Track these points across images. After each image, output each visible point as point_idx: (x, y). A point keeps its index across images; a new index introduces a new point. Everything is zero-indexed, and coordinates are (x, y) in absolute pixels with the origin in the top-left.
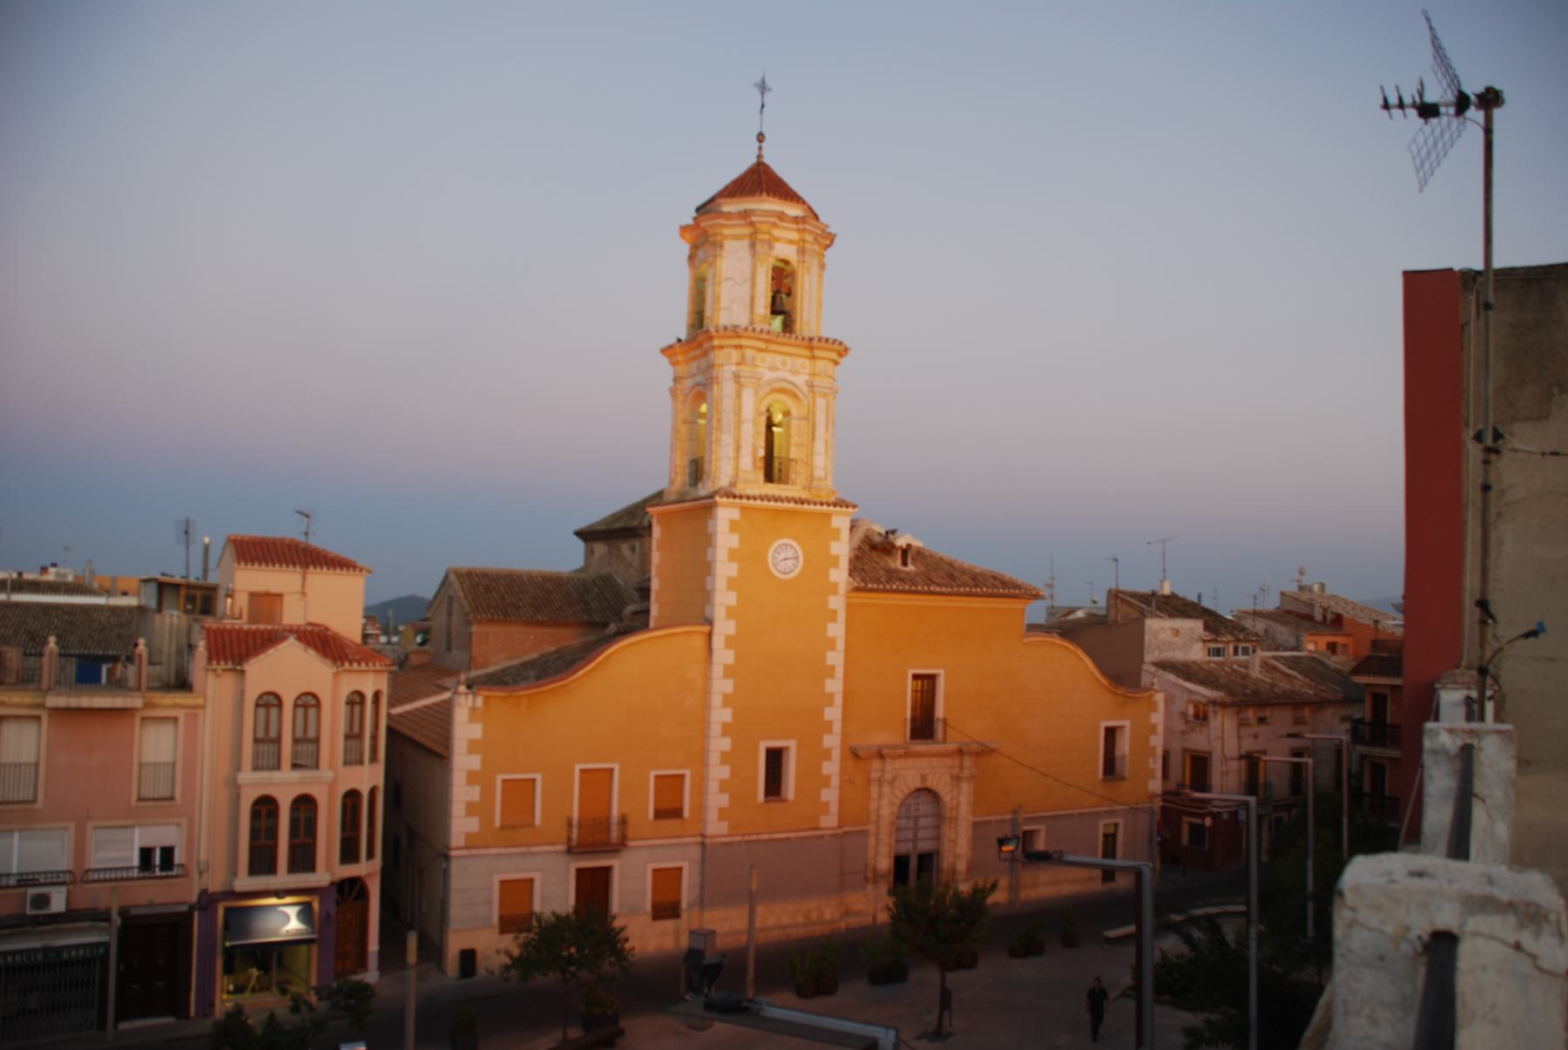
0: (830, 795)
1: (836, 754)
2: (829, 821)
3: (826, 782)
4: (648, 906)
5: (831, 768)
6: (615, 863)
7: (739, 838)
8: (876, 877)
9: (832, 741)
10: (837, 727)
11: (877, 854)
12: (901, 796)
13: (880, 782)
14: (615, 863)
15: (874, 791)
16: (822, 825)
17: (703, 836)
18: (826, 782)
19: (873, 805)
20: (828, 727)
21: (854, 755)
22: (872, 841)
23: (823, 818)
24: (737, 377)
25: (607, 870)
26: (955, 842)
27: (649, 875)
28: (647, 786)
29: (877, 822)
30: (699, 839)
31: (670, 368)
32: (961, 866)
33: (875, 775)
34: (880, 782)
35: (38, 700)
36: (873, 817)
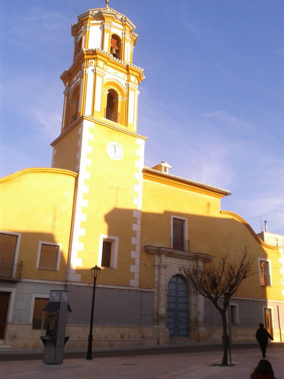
0: (135, 269)
1: (138, 248)
2: (134, 283)
3: (133, 262)
4: (31, 320)
5: (136, 255)
6: (14, 291)
7: (87, 285)
8: (158, 319)
9: (135, 241)
10: (138, 234)
11: (158, 306)
12: (170, 277)
13: (159, 267)
14: (14, 291)
15: (156, 271)
16: (131, 284)
17: (66, 281)
18: (133, 262)
19: (156, 279)
20: (134, 234)
21: (147, 251)
22: (156, 298)
23: (131, 281)
24: (94, 71)
25: (8, 294)
26: (196, 305)
27: (40, 246)
28: (37, 251)
29: (158, 288)
30: (63, 283)
31: (53, 147)
32: (201, 318)
33: (156, 263)
34: (159, 267)
35: (237, 284)
36: (156, 285)
